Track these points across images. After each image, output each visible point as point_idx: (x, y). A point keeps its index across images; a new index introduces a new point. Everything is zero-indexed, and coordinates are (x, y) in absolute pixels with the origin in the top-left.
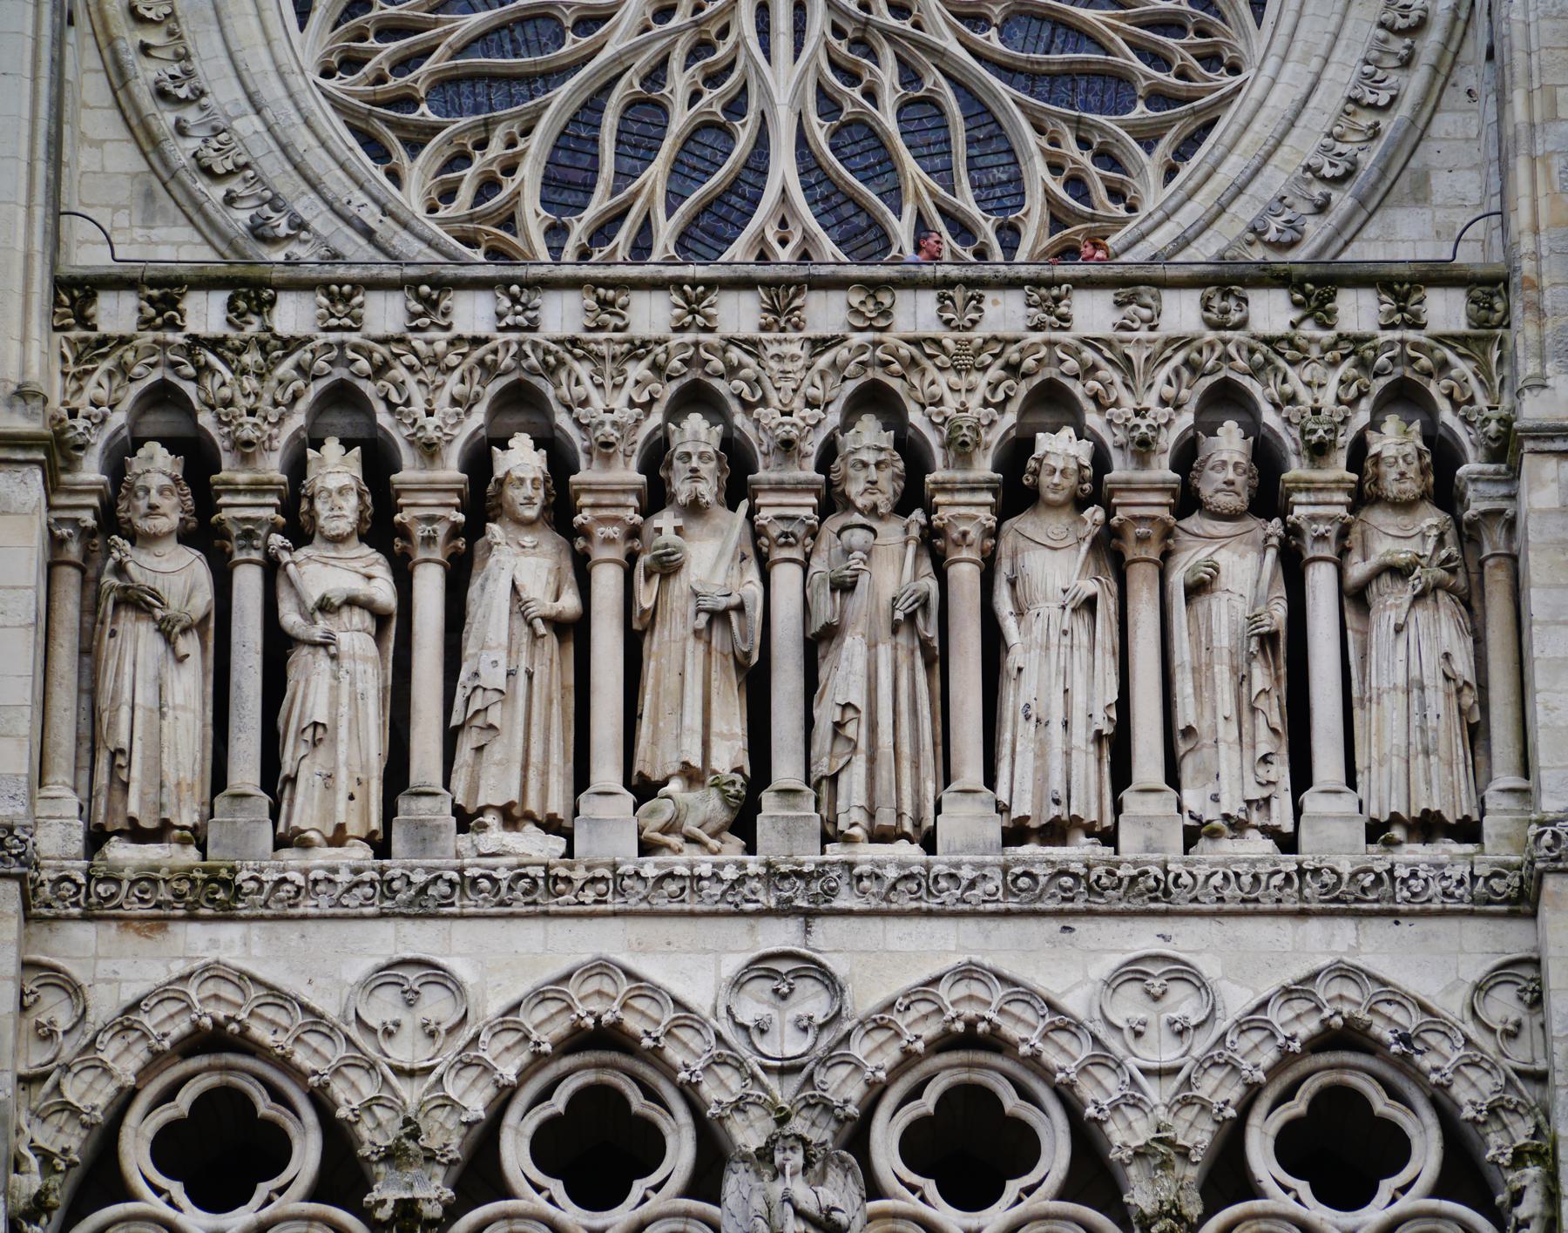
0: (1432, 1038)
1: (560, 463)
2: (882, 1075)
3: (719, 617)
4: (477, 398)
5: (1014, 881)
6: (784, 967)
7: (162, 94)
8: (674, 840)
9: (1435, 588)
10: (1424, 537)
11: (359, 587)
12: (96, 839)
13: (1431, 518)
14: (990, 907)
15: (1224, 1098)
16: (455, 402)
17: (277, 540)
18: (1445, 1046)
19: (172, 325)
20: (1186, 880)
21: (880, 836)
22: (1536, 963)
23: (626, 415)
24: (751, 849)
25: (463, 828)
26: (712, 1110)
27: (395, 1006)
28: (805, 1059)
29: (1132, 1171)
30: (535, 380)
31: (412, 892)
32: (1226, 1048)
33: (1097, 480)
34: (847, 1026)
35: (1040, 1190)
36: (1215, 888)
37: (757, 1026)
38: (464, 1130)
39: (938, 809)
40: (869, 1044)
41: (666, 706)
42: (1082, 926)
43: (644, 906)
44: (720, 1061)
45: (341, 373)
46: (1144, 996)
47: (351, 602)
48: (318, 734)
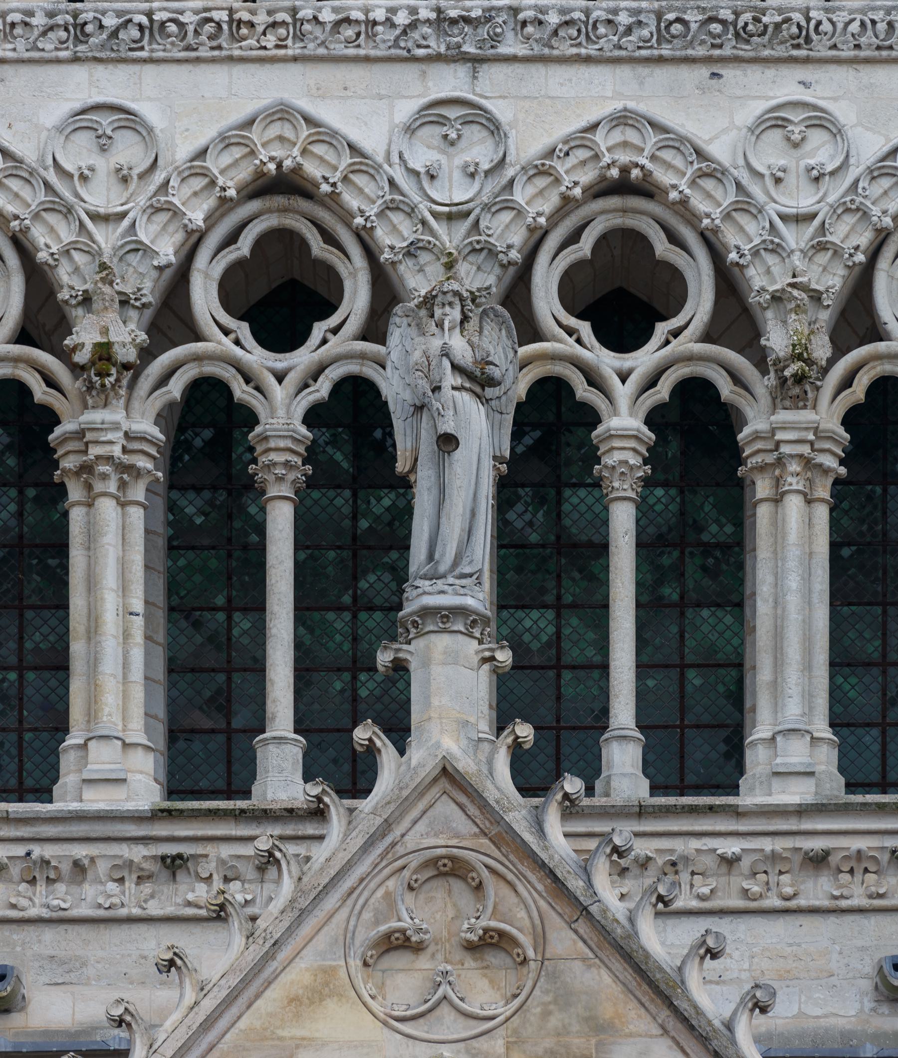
2: (542, 220)
5: (668, 27)
6: (452, 113)
14: (644, 53)
15: (855, 244)
20: (826, 27)
26: (386, 256)
27: (89, 150)
28: (471, 205)
29: (769, 314)
31: (104, 36)
32: (857, 194)
34: (510, 172)
35: (686, 333)
36: (853, 35)
37: (428, 172)
38: (154, 274)
40: (531, 190)
42: (729, 73)
43: (322, 51)
44: (391, 207)
46: (785, 142)
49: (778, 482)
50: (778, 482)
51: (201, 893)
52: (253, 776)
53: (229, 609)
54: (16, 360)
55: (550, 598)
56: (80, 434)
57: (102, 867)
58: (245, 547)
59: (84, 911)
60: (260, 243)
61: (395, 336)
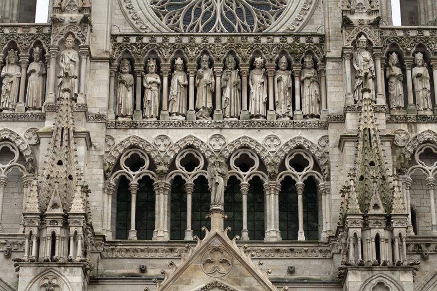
0: (312, 147)
1: (185, 62)
3: (208, 85)
4: (173, 52)
6: (217, 136)
7: (127, 8)
8: (201, 118)
9: (314, 81)
10: (312, 73)
11: (154, 80)
12: (117, 117)
13: (313, 71)
16: (169, 53)
17: (143, 73)
18: (314, 148)
19: (128, 41)
21: (232, 117)
22: (328, 136)
23: (194, 55)
24: (213, 119)
25: (170, 116)
30: (181, 50)
33: (264, 65)
34: (226, 145)
39: (240, 113)
40: (230, 148)
41: (200, 98)
42: (261, 130)
45: (153, 49)
47: (154, 82)
48: (149, 102)
49: (270, 192)
50: (270, 192)
51: (176, 254)
52: (185, 237)
53: (181, 211)
54: (148, 173)
55: (233, 210)
56: (158, 184)
57: (160, 250)
58: (184, 202)
59: (157, 257)
60: (186, 156)
61: (208, 169)
